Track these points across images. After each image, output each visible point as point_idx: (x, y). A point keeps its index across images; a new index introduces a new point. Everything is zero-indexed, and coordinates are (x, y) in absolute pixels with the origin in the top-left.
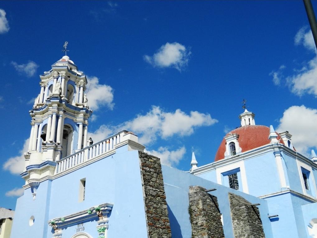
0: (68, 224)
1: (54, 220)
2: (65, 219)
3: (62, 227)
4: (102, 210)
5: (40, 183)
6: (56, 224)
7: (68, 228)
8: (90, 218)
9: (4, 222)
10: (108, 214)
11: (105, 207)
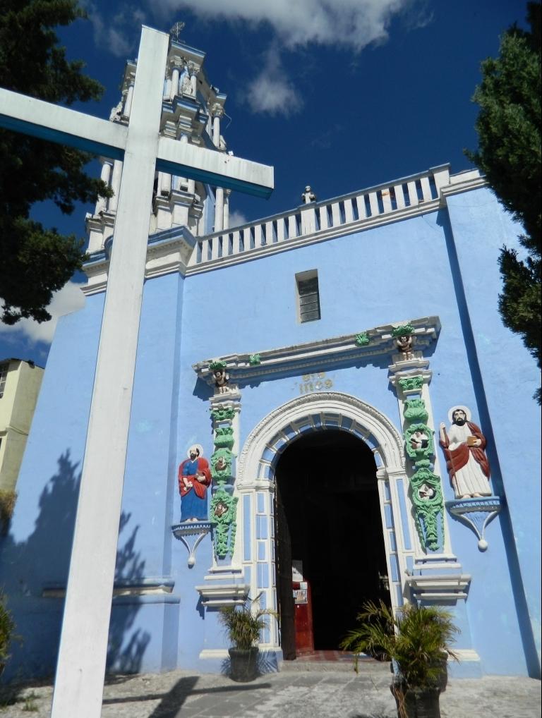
0: (266, 372)
1: (222, 359)
2: (262, 359)
3: (241, 380)
4: (418, 335)
6: (227, 371)
7: (264, 384)
9: (16, 368)
10: (427, 348)
11: (427, 328)
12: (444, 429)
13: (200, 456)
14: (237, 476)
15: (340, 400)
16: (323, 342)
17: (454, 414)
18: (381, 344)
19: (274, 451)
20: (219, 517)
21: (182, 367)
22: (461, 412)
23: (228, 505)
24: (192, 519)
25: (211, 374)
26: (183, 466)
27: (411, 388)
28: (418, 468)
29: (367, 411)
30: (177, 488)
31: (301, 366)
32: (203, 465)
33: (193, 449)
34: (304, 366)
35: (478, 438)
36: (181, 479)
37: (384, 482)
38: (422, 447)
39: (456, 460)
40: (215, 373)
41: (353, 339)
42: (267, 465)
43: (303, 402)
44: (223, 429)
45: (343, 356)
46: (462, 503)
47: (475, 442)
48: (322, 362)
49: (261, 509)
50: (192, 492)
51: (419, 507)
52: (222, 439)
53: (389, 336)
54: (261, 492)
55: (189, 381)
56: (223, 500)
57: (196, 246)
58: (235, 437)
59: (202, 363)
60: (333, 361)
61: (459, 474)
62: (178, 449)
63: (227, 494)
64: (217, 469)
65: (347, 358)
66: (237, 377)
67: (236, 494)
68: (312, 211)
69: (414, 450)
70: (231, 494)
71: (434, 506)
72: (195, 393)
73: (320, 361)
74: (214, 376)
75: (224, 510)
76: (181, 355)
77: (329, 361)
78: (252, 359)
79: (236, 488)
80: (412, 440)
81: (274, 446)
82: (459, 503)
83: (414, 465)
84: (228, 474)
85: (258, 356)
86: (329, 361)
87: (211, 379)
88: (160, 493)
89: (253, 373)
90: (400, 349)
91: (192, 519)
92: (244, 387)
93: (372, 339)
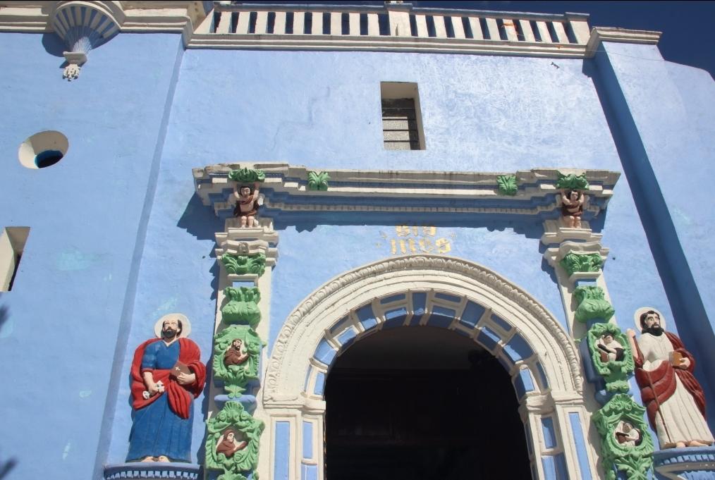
0: (332, 209)
1: (258, 166)
3: (281, 213)
5: (120, 31)
6: (265, 191)
7: (322, 229)
8: (488, 212)
12: (634, 337)
13: (182, 336)
14: (265, 381)
15: (465, 273)
16: (445, 176)
17: (643, 318)
18: (534, 198)
19: (335, 347)
20: (228, 457)
21: (161, 177)
22: (656, 315)
23: (249, 435)
24: (156, 458)
25: (231, 191)
26: (143, 350)
27: (585, 268)
28: (611, 394)
29: (513, 297)
30: (124, 391)
31: (397, 210)
32: (188, 352)
33: (172, 320)
34: (403, 210)
35: (684, 355)
36: (137, 374)
37: (539, 417)
38: (617, 360)
39: (654, 389)
40: (240, 188)
41: (493, 182)
42: (321, 371)
43: (400, 268)
44: (244, 290)
45: (471, 206)
46: (676, 455)
47: (682, 361)
48: (434, 210)
49: (307, 453)
50: (163, 402)
51: (619, 458)
52: (237, 307)
53: (551, 187)
54: (309, 418)
55: (175, 198)
56: (239, 423)
57: (211, 14)
58: (263, 307)
59: (214, 165)
60: (453, 210)
61: (664, 407)
62: (136, 316)
63: (245, 414)
64: (227, 362)
65: (476, 211)
66: (276, 207)
67: (259, 415)
68: (405, 16)
69: (606, 364)
70: (251, 412)
71: (644, 457)
72: (183, 223)
73: (431, 206)
74: (237, 194)
75: (237, 444)
76: (163, 157)
77: (447, 210)
78: (315, 179)
79: (259, 405)
80: (600, 346)
81: (335, 338)
82: (669, 456)
83: (605, 388)
84: (252, 375)
85: (326, 176)
86: (447, 210)
87: (226, 200)
88: (90, 395)
89: (313, 204)
90: (565, 210)
91: (156, 458)
92: (284, 228)
93: (522, 187)
